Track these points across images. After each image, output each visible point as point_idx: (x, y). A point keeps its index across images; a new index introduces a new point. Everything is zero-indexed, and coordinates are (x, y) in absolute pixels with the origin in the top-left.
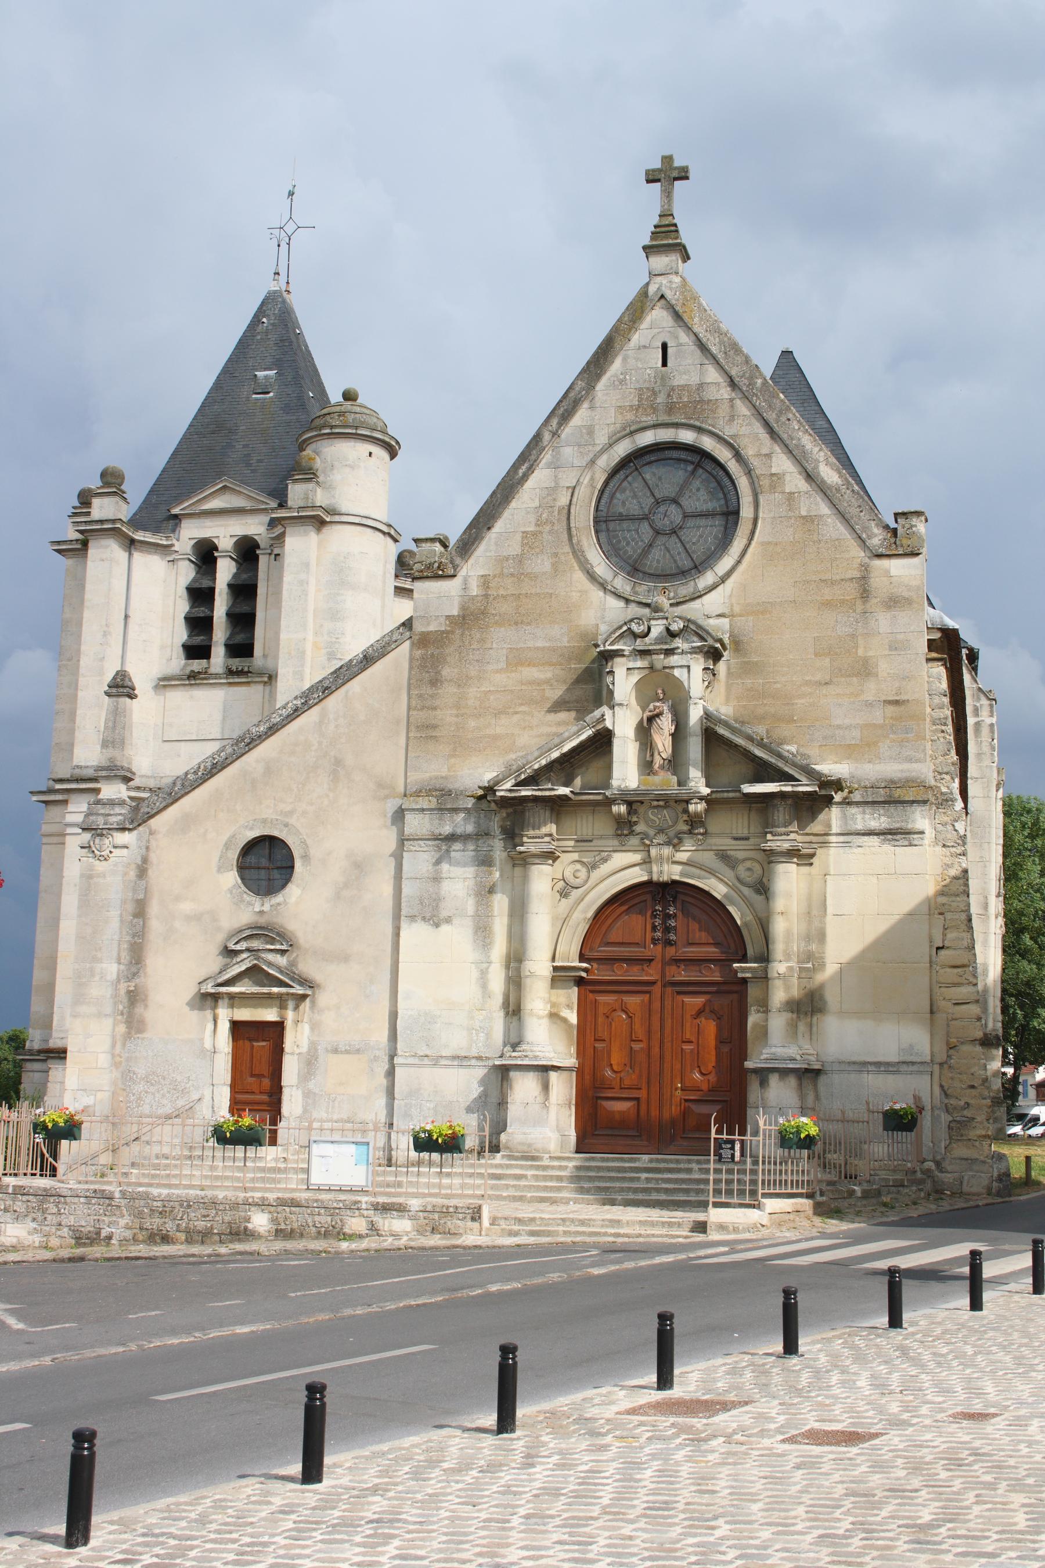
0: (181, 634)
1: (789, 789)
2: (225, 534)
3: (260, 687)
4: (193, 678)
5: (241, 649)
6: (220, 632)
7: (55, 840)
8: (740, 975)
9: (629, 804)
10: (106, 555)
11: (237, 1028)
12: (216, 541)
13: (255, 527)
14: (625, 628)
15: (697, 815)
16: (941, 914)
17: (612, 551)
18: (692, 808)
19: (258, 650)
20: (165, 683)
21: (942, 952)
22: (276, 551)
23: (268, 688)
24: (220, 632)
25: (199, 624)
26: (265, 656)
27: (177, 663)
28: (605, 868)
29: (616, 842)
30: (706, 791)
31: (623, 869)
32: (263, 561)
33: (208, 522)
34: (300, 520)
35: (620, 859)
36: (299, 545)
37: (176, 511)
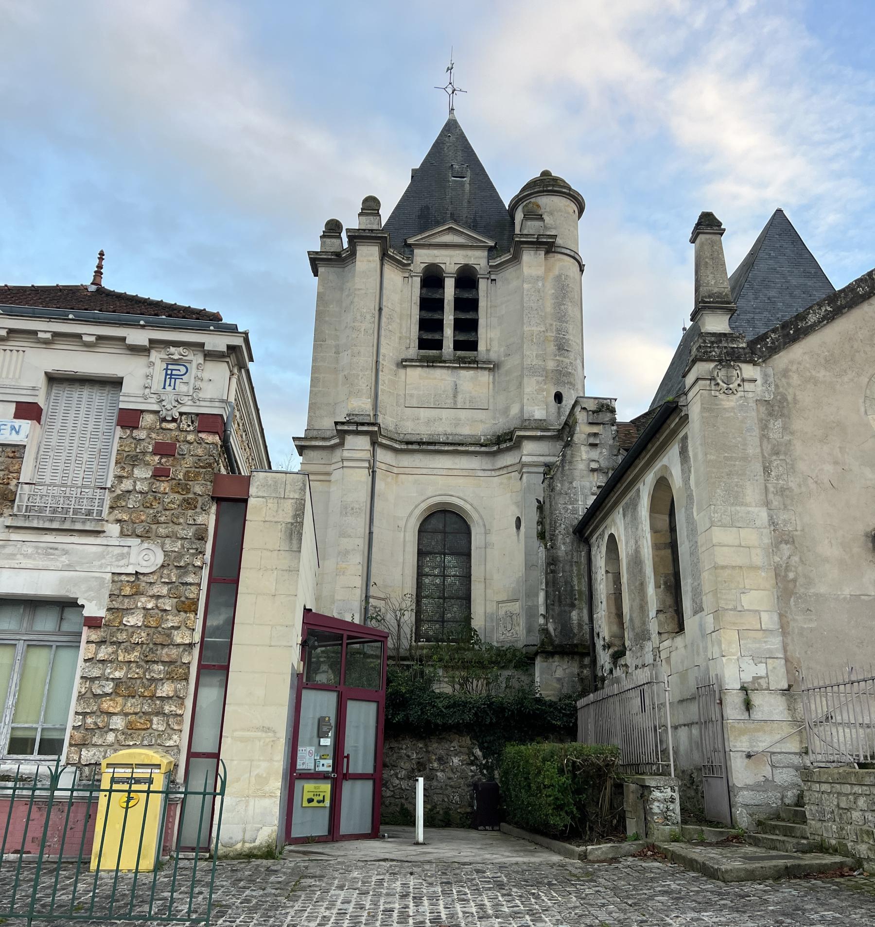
2: (451, 261)
3: (486, 373)
5: (467, 342)
12: (443, 266)
13: (478, 259)
19: (481, 347)
22: (493, 277)
23: (491, 374)
26: (488, 351)
27: (413, 351)
32: (483, 284)
33: (436, 252)
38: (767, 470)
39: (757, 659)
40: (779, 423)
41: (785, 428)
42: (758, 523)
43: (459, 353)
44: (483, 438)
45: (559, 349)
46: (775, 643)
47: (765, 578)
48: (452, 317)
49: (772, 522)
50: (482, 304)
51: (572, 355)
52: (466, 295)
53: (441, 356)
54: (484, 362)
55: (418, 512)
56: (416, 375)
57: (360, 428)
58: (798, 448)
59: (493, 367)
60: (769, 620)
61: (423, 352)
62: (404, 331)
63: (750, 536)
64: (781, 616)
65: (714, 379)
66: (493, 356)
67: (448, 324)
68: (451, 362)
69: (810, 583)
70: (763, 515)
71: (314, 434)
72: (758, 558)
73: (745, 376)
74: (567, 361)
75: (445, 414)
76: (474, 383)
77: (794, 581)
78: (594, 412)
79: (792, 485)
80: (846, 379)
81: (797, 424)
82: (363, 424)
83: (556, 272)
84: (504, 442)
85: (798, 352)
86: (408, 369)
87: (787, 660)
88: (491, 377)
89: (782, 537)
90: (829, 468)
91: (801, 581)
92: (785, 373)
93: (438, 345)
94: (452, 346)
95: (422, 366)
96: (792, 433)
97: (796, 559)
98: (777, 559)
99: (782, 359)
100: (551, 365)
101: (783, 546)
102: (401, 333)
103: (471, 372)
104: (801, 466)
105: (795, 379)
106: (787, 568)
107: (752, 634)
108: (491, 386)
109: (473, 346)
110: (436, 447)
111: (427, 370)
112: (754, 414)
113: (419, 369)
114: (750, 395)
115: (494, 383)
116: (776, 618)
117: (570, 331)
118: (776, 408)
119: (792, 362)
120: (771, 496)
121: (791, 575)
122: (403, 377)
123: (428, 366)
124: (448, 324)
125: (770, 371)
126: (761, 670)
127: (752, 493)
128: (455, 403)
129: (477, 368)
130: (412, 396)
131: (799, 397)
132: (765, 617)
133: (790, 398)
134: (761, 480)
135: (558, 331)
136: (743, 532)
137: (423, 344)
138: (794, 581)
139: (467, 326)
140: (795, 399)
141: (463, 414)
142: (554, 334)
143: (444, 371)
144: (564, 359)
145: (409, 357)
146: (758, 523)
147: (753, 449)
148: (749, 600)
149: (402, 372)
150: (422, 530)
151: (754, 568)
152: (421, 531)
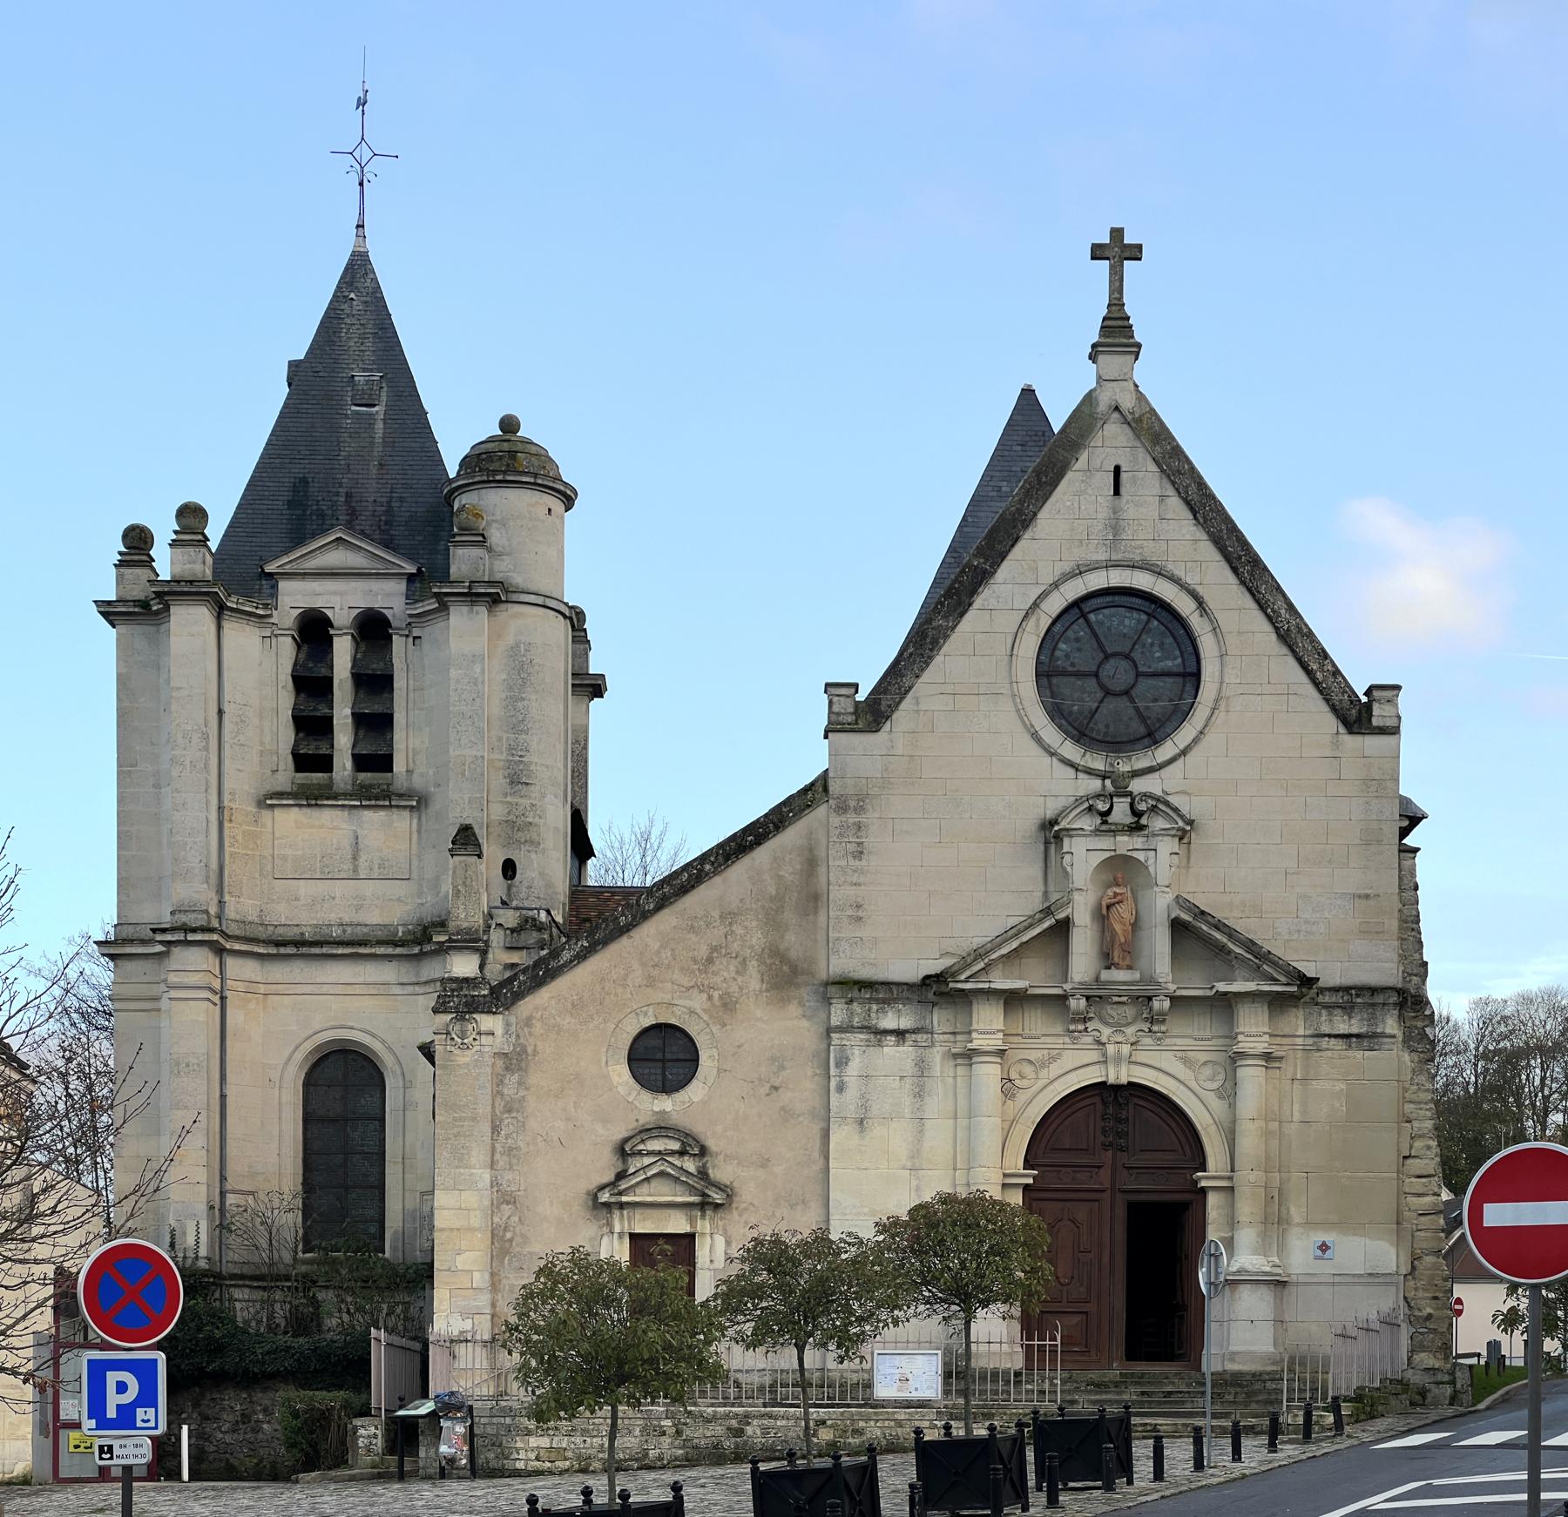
0: (286, 735)
1: (1267, 988)
3: (406, 813)
4: (310, 797)
5: (375, 761)
6: (344, 738)
7: (148, 1005)
8: (1203, 1184)
9: (1088, 998)
10: (190, 624)
11: (632, 1236)
14: (1086, 805)
15: (1161, 1013)
16: (1409, 1121)
17: (1056, 713)
18: (1156, 1004)
19: (399, 765)
20: (270, 800)
21: (1409, 1161)
23: (415, 815)
24: (344, 738)
25: (312, 725)
27: (286, 776)
28: (1055, 1069)
29: (1067, 1040)
30: (1172, 987)
31: (1068, 1065)
34: (471, 597)
35: (1070, 1059)
36: (465, 629)
37: (269, 568)
38: (496, 1129)
39: (465, 1315)
40: (515, 1078)
41: (520, 1083)
42: (480, 1186)
43: (362, 776)
44: (401, 929)
45: (512, 783)
46: (483, 1301)
47: (481, 1240)
48: (348, 711)
49: (494, 1183)
50: (399, 683)
51: (535, 791)
52: (376, 667)
53: (330, 785)
54: (401, 796)
55: (299, 1056)
56: (291, 822)
57: (191, 937)
58: (532, 1103)
59: (417, 802)
60: (480, 1279)
61: (302, 777)
62: (267, 739)
63: (470, 1198)
64: (492, 1275)
65: (448, 1033)
66: (417, 782)
67: (343, 730)
68: (346, 795)
69: (526, 1240)
70: (486, 1175)
71: (128, 932)
72: (476, 1220)
73: (483, 1028)
74: (526, 802)
75: (339, 888)
76: (383, 832)
77: (511, 1240)
78: (513, 931)
79: (521, 1144)
80: (591, 1026)
81: (534, 1078)
82: (194, 930)
83: (511, 640)
84: (422, 940)
85: (544, 997)
86: (277, 811)
87: (493, 1316)
88: (415, 821)
89: (504, 1198)
90: (560, 1124)
91: (518, 1240)
92: (528, 1022)
93: (324, 763)
94: (349, 764)
95: (300, 806)
96: (527, 1089)
97: (516, 1219)
98: (496, 1219)
99: (527, 1006)
100: (498, 812)
101: (504, 1206)
102: (262, 743)
103: (382, 813)
104: (533, 1124)
105: (538, 1028)
106: (506, 1229)
107: (464, 1292)
108: (415, 836)
109: (383, 763)
110: (325, 950)
111: (308, 810)
112: (489, 1070)
113: (296, 810)
114: (487, 1049)
115: (419, 832)
116: (487, 1276)
117: (533, 746)
118: (514, 1061)
119: (537, 1009)
120: (497, 1156)
121: (509, 1235)
122: (269, 824)
123: (309, 805)
124: (343, 730)
125: (513, 1019)
126: (468, 1325)
127: (478, 1156)
128: (355, 871)
129: (391, 806)
130: (284, 858)
131: (539, 1048)
132: (477, 1276)
133: (530, 1050)
134: (487, 1139)
135: (511, 749)
136: (465, 1195)
137: (303, 762)
138: (511, 1240)
139: (374, 724)
140: (535, 1052)
141: (369, 888)
142: (504, 757)
143: (338, 813)
144: (520, 801)
145: (279, 789)
146: (480, 1186)
147: (484, 1108)
148: (462, 1262)
149: (266, 814)
150: (309, 1083)
151: (471, 1230)
152: (307, 1084)
